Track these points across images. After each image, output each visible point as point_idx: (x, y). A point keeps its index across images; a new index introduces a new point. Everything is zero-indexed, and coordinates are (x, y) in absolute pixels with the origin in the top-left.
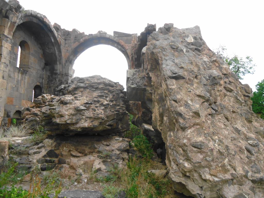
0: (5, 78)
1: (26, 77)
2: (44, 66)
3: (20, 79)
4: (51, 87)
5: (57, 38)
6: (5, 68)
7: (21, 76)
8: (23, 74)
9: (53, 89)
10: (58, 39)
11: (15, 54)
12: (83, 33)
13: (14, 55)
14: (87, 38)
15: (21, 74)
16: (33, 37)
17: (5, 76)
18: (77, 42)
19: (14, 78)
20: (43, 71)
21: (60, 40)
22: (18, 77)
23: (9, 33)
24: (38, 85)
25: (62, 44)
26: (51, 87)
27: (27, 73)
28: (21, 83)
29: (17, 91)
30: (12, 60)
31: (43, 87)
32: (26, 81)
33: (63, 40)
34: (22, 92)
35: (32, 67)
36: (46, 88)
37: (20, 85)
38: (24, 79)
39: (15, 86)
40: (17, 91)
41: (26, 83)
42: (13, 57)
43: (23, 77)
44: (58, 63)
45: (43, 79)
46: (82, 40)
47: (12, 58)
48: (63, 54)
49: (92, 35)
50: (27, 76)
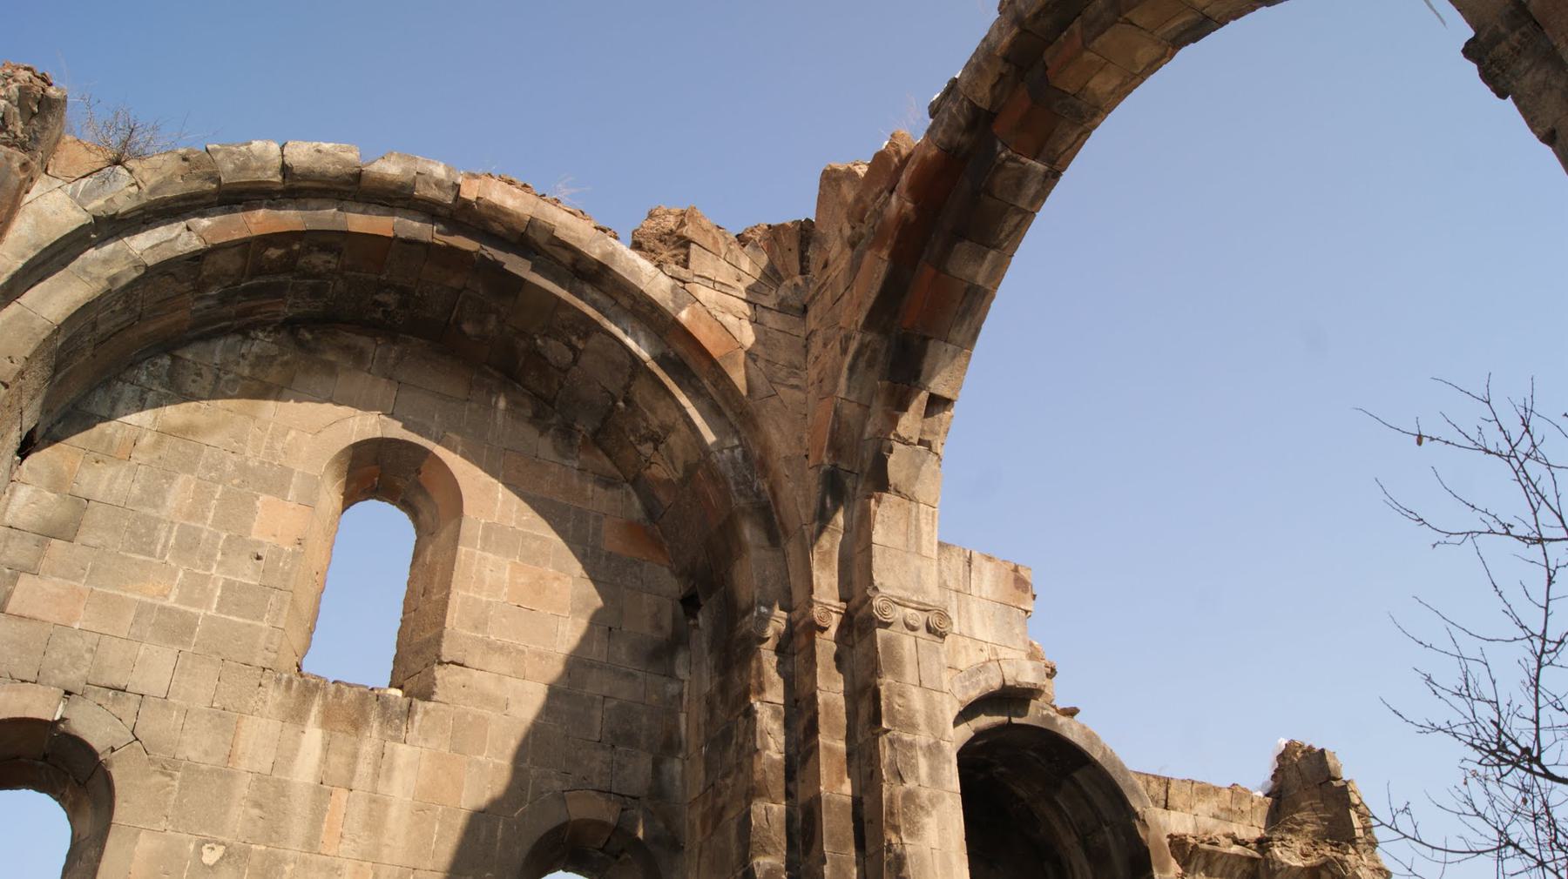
2: (667, 622)
4: (723, 808)
5: (670, 306)
7: (327, 748)
8: (357, 724)
9: (733, 833)
10: (684, 316)
11: (259, 558)
13: (249, 565)
15: (327, 721)
16: (502, 404)
18: (868, 256)
19: (226, 775)
20: (671, 675)
21: (729, 320)
22: (286, 757)
24: (603, 825)
26: (723, 808)
27: (409, 712)
30: (212, 612)
31: (676, 846)
32: (400, 790)
35: (491, 647)
36: (699, 838)
37: (311, 844)
39: (227, 855)
41: (398, 817)
42: (229, 587)
43: (355, 756)
44: (749, 533)
45: (670, 745)
47: (218, 593)
48: (780, 438)
50: (413, 733)
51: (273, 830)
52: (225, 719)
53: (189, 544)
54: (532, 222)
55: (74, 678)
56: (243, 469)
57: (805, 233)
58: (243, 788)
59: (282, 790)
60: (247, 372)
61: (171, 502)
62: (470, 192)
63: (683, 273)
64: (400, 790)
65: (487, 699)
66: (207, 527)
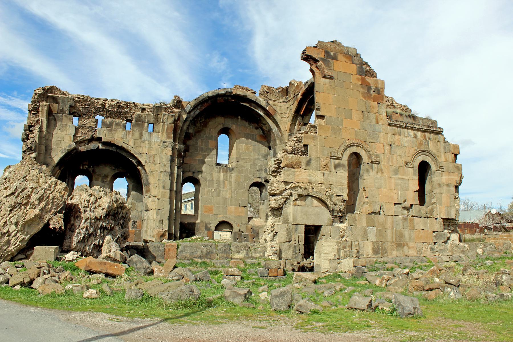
0: (166, 188)
1: (233, 175)
3: (221, 179)
5: (265, 107)
6: (165, 177)
7: (224, 176)
8: (227, 172)
12: (300, 83)
14: (304, 89)
15: (223, 172)
17: (165, 186)
18: (296, 102)
19: (213, 181)
21: (275, 107)
22: (219, 178)
23: (168, 137)
25: (278, 111)
27: (233, 169)
28: (224, 184)
29: (219, 196)
32: (233, 180)
33: (282, 105)
34: (228, 196)
37: (224, 188)
38: (228, 178)
40: (219, 196)
41: (233, 184)
44: (278, 142)
46: (300, 97)
49: (307, 82)
51: (219, 187)
52: (211, 174)
53: (202, 150)
54: (244, 96)
55: (193, 170)
56: (206, 137)
57: (287, 89)
58: (215, 182)
59: (219, 182)
60: (203, 120)
61: (199, 144)
62: (234, 93)
63: (268, 99)
64: (233, 180)
65: (242, 166)
66: (204, 147)
